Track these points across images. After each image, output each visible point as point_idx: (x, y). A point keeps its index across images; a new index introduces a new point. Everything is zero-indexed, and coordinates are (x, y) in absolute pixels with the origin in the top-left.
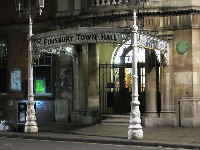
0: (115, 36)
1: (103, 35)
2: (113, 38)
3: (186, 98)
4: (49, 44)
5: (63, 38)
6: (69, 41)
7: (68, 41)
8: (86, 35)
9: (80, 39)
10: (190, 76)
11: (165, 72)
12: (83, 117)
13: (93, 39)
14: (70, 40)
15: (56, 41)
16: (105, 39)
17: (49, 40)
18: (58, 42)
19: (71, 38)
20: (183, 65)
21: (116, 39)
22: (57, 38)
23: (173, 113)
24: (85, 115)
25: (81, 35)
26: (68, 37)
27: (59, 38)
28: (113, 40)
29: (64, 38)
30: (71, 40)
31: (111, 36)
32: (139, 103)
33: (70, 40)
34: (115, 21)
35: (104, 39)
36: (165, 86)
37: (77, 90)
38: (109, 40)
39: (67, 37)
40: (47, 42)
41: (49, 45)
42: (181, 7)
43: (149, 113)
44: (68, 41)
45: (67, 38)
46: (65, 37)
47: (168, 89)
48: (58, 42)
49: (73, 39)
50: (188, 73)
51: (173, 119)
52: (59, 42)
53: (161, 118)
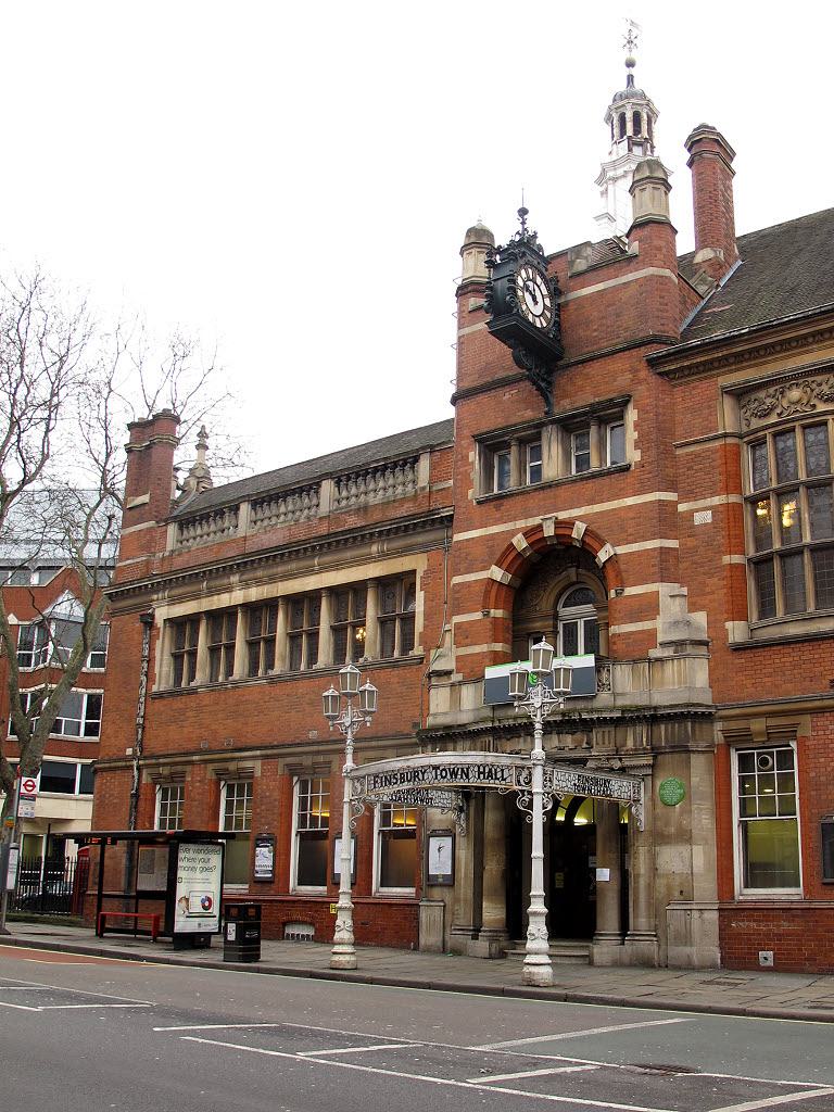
0: (502, 770)
1: (481, 770)
9: (439, 777)
10: (686, 854)
12: (471, 942)
19: (423, 774)
20: (673, 830)
23: (655, 936)
24: (475, 937)
35: (482, 776)
36: (637, 876)
42: (665, 707)
43: (601, 935)
47: (642, 882)
50: (684, 849)
51: (648, 947)
53: (628, 947)
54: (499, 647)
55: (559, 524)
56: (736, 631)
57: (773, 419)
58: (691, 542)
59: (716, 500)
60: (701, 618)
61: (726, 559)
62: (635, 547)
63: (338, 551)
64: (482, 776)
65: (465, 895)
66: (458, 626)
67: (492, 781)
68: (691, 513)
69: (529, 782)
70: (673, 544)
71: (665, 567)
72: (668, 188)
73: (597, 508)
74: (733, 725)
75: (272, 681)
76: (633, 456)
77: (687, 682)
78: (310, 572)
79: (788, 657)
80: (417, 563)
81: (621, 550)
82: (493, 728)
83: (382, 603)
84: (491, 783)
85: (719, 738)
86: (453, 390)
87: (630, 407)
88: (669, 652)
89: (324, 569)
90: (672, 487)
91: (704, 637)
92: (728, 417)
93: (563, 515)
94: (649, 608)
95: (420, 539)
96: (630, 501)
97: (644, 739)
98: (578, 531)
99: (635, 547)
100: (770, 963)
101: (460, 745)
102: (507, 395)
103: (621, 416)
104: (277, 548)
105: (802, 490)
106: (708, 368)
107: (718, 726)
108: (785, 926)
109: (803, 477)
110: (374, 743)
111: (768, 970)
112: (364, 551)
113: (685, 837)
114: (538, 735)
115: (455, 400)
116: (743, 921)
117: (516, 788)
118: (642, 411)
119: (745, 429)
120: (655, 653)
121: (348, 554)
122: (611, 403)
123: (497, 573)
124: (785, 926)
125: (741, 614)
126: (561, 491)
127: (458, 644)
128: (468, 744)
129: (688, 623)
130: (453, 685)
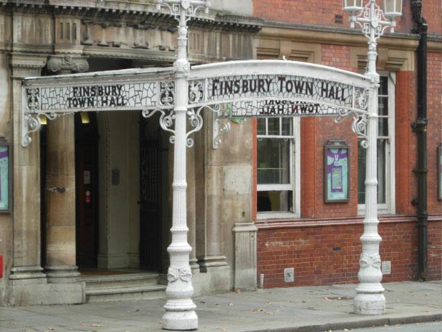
0: (343, 90)
1: (325, 87)
2: (340, 94)
3: (242, 226)
4: (221, 93)
5: (251, 81)
6: (264, 91)
7: (261, 89)
8: (295, 82)
9: (284, 90)
11: (210, 163)
13: (306, 93)
14: (266, 89)
15: (236, 89)
16: (327, 96)
17: (222, 83)
18: (241, 89)
19: (269, 84)
21: (344, 98)
22: (239, 81)
25: (287, 79)
26: (262, 80)
27: (244, 81)
28: (339, 99)
29: (253, 82)
30: (268, 90)
31: (337, 88)
32: (380, 238)
33: (266, 89)
34: (141, 29)
35: (324, 93)
37: (24, 209)
38: (333, 98)
39: (260, 81)
40: (219, 87)
41: (222, 96)
44: (261, 89)
45: (259, 83)
46: (255, 81)
48: (241, 89)
49: (271, 85)
52: (244, 92)
64: (324, 93)
65: (28, 224)
67: (333, 100)
97: (218, 48)
100: (292, 279)
108: (303, 243)
111: (291, 285)
116: (274, 240)
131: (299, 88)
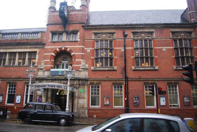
20: (81, 97)
36: (75, 104)
50: (83, 100)
54: (52, 66)
55: (65, 48)
56: (92, 68)
57: (100, 38)
58: (86, 54)
59: (91, 49)
60: (87, 65)
61: (92, 57)
62: (78, 53)
63: (21, 46)
66: (45, 62)
68: (87, 50)
69: (67, 89)
70: (84, 54)
71: (82, 57)
72: (56, 3)
73: (72, 46)
74: (91, 82)
75: (5, 66)
76: (78, 39)
77: (83, 75)
78: (15, 48)
79: (100, 73)
80: (38, 50)
81: (75, 54)
82: (52, 79)
83: (29, 56)
84: (59, 88)
85: (89, 83)
86: (47, 23)
87: (79, 32)
88: (82, 70)
89: (18, 48)
90: (84, 45)
91: (88, 68)
92: (93, 37)
93: (66, 47)
94: (79, 63)
95: (38, 46)
96: (77, 46)
98: (68, 50)
99: (78, 53)
101: (44, 81)
102: (58, 26)
103: (77, 33)
104: (9, 43)
105: (104, 49)
106: (91, 29)
107: (89, 82)
108: (98, 111)
109: (104, 47)
110: (26, 79)
112: (27, 47)
113: (83, 98)
114: (69, 81)
115: (47, 25)
117: (64, 89)
118: (80, 33)
119: (96, 39)
120: (81, 70)
121: (23, 47)
122: (76, 31)
123: (53, 54)
124: (98, 111)
125: (93, 66)
126: (66, 43)
127: (45, 64)
128: (46, 81)
129: (86, 66)
130: (43, 71)
131: (52, 86)
